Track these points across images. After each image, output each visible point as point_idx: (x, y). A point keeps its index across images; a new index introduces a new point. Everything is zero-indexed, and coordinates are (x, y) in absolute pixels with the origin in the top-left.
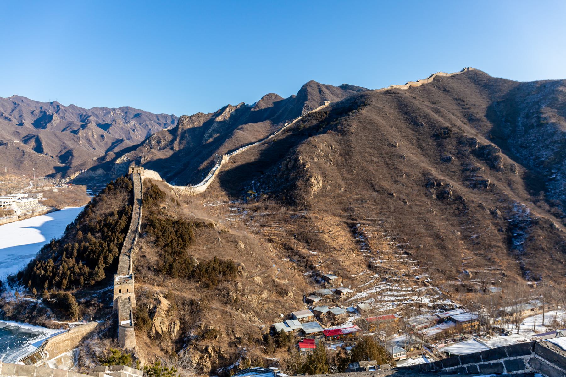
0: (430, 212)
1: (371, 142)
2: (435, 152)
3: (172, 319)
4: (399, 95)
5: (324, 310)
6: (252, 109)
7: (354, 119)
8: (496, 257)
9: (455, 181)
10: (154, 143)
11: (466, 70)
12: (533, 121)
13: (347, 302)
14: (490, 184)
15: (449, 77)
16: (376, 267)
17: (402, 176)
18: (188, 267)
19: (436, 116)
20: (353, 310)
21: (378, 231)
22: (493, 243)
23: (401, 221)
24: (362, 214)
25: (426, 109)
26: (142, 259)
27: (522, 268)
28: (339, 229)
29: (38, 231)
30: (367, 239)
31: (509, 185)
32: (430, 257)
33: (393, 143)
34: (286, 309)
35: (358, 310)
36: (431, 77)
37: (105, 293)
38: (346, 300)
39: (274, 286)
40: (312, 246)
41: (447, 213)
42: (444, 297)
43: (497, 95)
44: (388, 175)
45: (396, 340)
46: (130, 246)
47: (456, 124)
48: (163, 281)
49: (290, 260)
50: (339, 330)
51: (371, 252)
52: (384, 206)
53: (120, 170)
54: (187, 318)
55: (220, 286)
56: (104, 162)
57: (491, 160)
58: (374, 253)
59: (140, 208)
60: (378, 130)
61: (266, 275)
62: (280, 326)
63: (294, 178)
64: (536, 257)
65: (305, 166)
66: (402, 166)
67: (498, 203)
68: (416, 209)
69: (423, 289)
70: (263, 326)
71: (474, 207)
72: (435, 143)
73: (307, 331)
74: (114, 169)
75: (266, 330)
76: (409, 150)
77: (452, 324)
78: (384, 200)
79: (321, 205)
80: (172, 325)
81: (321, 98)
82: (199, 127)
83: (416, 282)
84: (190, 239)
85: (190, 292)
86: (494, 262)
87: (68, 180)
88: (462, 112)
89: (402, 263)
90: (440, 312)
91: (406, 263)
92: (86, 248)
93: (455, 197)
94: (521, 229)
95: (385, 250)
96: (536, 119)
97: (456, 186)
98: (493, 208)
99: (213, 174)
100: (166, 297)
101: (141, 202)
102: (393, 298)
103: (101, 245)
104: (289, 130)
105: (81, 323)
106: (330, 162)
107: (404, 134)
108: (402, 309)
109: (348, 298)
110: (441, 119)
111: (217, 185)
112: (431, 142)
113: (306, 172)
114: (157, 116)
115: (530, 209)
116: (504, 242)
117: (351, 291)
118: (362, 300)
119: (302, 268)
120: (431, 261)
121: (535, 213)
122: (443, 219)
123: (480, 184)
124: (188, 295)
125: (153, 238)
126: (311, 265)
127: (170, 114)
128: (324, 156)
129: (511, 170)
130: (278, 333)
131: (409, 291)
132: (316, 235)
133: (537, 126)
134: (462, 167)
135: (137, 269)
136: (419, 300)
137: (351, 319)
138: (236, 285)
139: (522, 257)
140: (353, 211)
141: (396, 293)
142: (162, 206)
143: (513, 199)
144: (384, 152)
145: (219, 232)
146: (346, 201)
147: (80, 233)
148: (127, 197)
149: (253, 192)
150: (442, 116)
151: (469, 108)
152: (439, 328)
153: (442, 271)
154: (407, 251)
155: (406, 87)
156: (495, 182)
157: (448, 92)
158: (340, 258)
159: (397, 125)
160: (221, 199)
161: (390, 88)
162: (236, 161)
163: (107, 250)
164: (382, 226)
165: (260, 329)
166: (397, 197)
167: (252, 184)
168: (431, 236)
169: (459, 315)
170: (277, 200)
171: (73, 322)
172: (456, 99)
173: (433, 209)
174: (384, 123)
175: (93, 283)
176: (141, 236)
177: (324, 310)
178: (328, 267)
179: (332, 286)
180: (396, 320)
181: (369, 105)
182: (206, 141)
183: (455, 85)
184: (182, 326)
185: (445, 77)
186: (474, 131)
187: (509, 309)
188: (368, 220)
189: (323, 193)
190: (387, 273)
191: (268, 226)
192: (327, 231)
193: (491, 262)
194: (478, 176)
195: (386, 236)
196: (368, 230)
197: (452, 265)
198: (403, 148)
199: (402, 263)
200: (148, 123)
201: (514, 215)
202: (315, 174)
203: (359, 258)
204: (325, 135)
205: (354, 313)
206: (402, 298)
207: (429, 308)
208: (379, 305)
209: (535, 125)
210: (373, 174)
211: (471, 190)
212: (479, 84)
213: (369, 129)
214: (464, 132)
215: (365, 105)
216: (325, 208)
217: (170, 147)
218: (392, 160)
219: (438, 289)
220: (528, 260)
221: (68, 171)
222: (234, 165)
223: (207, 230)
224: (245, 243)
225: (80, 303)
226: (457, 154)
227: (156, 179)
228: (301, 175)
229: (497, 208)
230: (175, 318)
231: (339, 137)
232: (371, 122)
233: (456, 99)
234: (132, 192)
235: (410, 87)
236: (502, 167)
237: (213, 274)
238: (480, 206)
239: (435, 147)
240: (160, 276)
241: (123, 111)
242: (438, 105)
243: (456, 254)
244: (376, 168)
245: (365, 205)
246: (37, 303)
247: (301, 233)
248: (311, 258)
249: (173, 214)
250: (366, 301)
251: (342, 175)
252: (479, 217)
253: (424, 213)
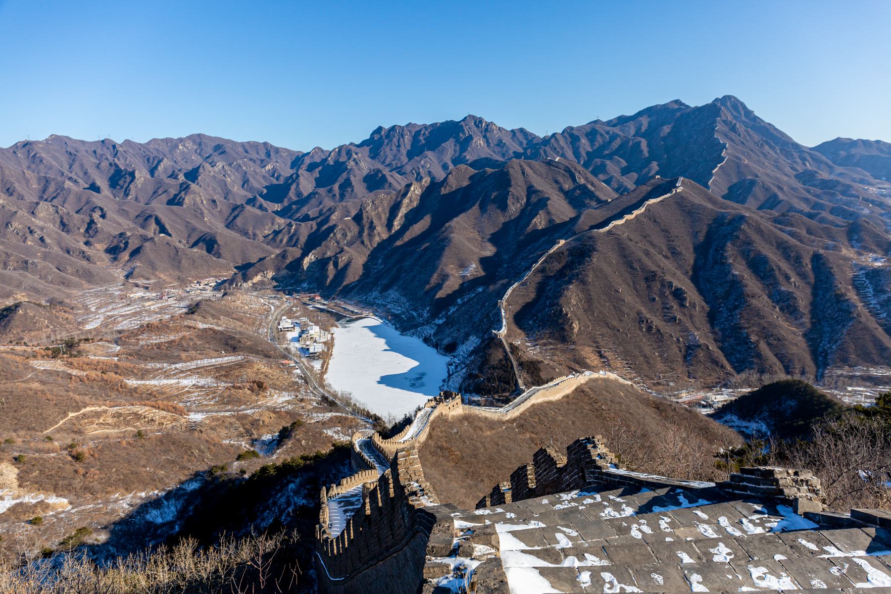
0: (642, 341)
10: (339, 236)
31: (691, 318)
32: (642, 369)
66: (624, 309)
87: (250, 283)
97: (657, 322)
98: (678, 335)
112: (643, 284)
114: (242, 145)
127: (261, 141)
172: (663, 231)
193: (673, 369)
196: (608, 354)
231: (581, 286)
232: (601, 271)
233: (663, 231)
234: (504, 348)
238: (671, 335)
241: (194, 142)
252: (669, 343)
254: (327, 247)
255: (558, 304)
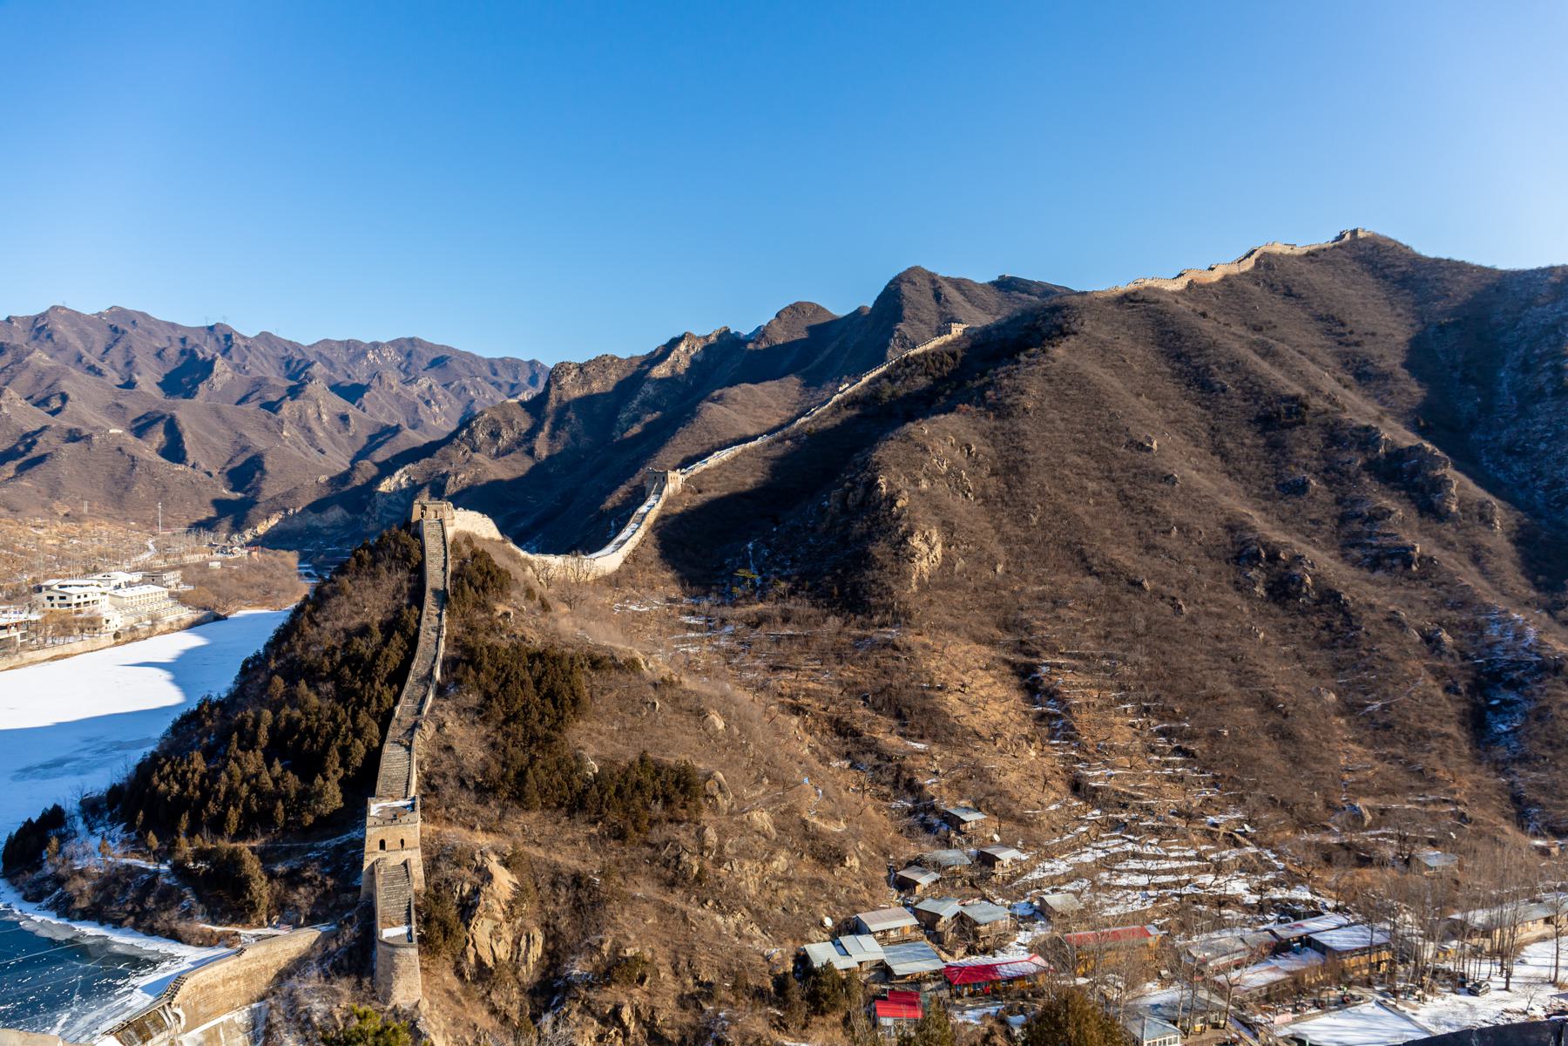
0: (1250, 633)
1: (1081, 436)
2: (1263, 464)
3: (522, 926)
4: (1159, 307)
5: (948, 910)
6: (750, 346)
7: (1032, 373)
8: (1439, 765)
9: (1319, 548)
10: (481, 436)
11: (1348, 237)
12: (1543, 379)
13: (1011, 887)
14: (1421, 557)
15: (1299, 258)
16: (1096, 789)
17: (1169, 532)
18: (569, 780)
19: (1265, 366)
20: (1028, 912)
21: (1100, 687)
22: (1432, 726)
23: (1166, 659)
24: (1056, 638)
25: (1236, 345)
26: (443, 756)
27: (1516, 799)
28: (991, 680)
29: (165, 675)
30: (1068, 710)
31: (1476, 560)
32: (1248, 764)
33: (1142, 439)
34: (838, 903)
35: (1042, 912)
36: (1249, 256)
37: (340, 849)
38: (1009, 882)
39: (806, 837)
40: (913, 727)
41: (1297, 638)
42: (1292, 880)
43: (1438, 306)
44: (1127, 529)
45: (1154, 1001)
46: (411, 720)
47: (1322, 387)
48: (501, 818)
49: (851, 766)
50: (990, 969)
51: (1081, 747)
52: (1117, 617)
53: (389, 511)
54: (564, 923)
55: (656, 835)
56: (348, 487)
57: (1422, 490)
58: (1090, 750)
59: (440, 616)
60: (1098, 405)
61: (784, 806)
62: (821, 952)
63: (862, 536)
64: (1557, 768)
65: (893, 502)
67: (1444, 612)
68: (1207, 626)
69: (1231, 854)
70: (775, 952)
71: (1375, 622)
72: (1262, 442)
73: (899, 968)
74: (373, 508)
75: (782, 962)
76: (1188, 460)
77: (1313, 957)
78: (1117, 600)
79: (940, 613)
80: (523, 943)
81: (941, 314)
82: (605, 395)
83: (1210, 835)
84: (575, 701)
85: (572, 850)
86: (1433, 779)
88: (1338, 355)
89: (1170, 779)
90: (1280, 921)
91: (1182, 779)
92: (292, 725)
93: (1320, 593)
94: (1512, 685)
95: (1120, 743)
96: (1549, 374)
97: (1321, 562)
98: (1429, 626)
99: (640, 524)
100: (506, 864)
101: (443, 598)
102: (1143, 880)
103: (333, 718)
104: (852, 401)
105: (274, 932)
106: (965, 491)
107: (1173, 415)
108: (1169, 912)
109: (1013, 878)
110: (1277, 375)
111: (652, 552)
112: (1249, 437)
113: (898, 518)
114: (491, 363)
115: (1535, 629)
116: (1462, 723)
117: (1024, 857)
118: (1055, 883)
119: (886, 790)
120: (1252, 774)
121: (1553, 641)
122: (1285, 655)
123: (1392, 557)
124: (568, 860)
125: (474, 699)
126: (911, 781)
127: (527, 359)
128: (948, 474)
129: (1482, 517)
130: (815, 972)
131: (1190, 859)
132: (924, 696)
133: (1555, 393)
134: (1340, 510)
135: (428, 784)
136: (1219, 886)
137: (1023, 937)
138: (700, 834)
139: (1516, 768)
140: (1029, 629)
141: (1150, 865)
142: (501, 608)
143: (1487, 600)
144: (1116, 465)
145: (655, 685)
146: (1010, 601)
147: (278, 681)
148: (405, 585)
149: (749, 574)
150: (1281, 365)
151: (1357, 344)
152: (1276, 969)
153: (1283, 804)
154: (1184, 746)
155: (1180, 285)
156: (1436, 552)
157: (1299, 297)
158: (993, 763)
159: (1153, 388)
160: (661, 592)
161: (1132, 287)
162: (704, 486)
163: (348, 729)
164: (1111, 672)
165: (767, 959)
166: (1155, 591)
167: (747, 550)
168: (1250, 702)
169: (1332, 930)
170: (817, 597)
171: (252, 927)
172: (1320, 318)
173: (1257, 628)
174: (1117, 383)
175: (309, 819)
176: (441, 692)
177: (948, 910)
178: (957, 786)
179: (969, 841)
180: (1151, 941)
181: (1075, 333)
182: (624, 431)
183: (1318, 278)
184: (550, 946)
185: (1289, 256)
186: (1372, 408)
187: (1479, 917)
188: (1071, 656)
189: (945, 579)
190: (1125, 806)
191: (791, 670)
192: (955, 685)
194: (1386, 535)
195: (1122, 700)
196: (1072, 683)
197: (1313, 787)
198: (1170, 453)
199: (1170, 779)
200: (467, 382)
201: (1490, 646)
202: (923, 526)
203: (1047, 762)
204: (952, 417)
205: (1031, 918)
206: (1171, 878)
207: (1248, 908)
208: (1103, 898)
209: (1548, 390)
210: (1086, 527)
211: (1365, 573)
212: (1385, 277)
213: (1074, 401)
214: (1344, 410)
215: (1064, 334)
216: (950, 620)
217: (524, 447)
218: (1137, 486)
219: (1272, 856)
220: (1534, 775)
221: (251, 512)
222: (699, 499)
223: (621, 678)
224: (726, 716)
225: (272, 876)
226: (1326, 471)
227: (486, 536)
228: (883, 526)
229: (1440, 624)
230: (530, 923)
231: (990, 423)
233: (1320, 318)
234: (420, 570)
235: (1191, 283)
236: (1454, 508)
237: (637, 802)
239: (1260, 451)
240: (492, 804)
241: (400, 350)
242: (1271, 333)
243: (1325, 755)
244: (1092, 510)
245: (1063, 612)
246: (157, 873)
247: (883, 691)
248: (909, 762)
249: (530, 633)
250: (1069, 887)
251: (998, 529)
252: (1388, 649)
253: (1231, 638)
254: (445, 458)
255: (865, 466)
